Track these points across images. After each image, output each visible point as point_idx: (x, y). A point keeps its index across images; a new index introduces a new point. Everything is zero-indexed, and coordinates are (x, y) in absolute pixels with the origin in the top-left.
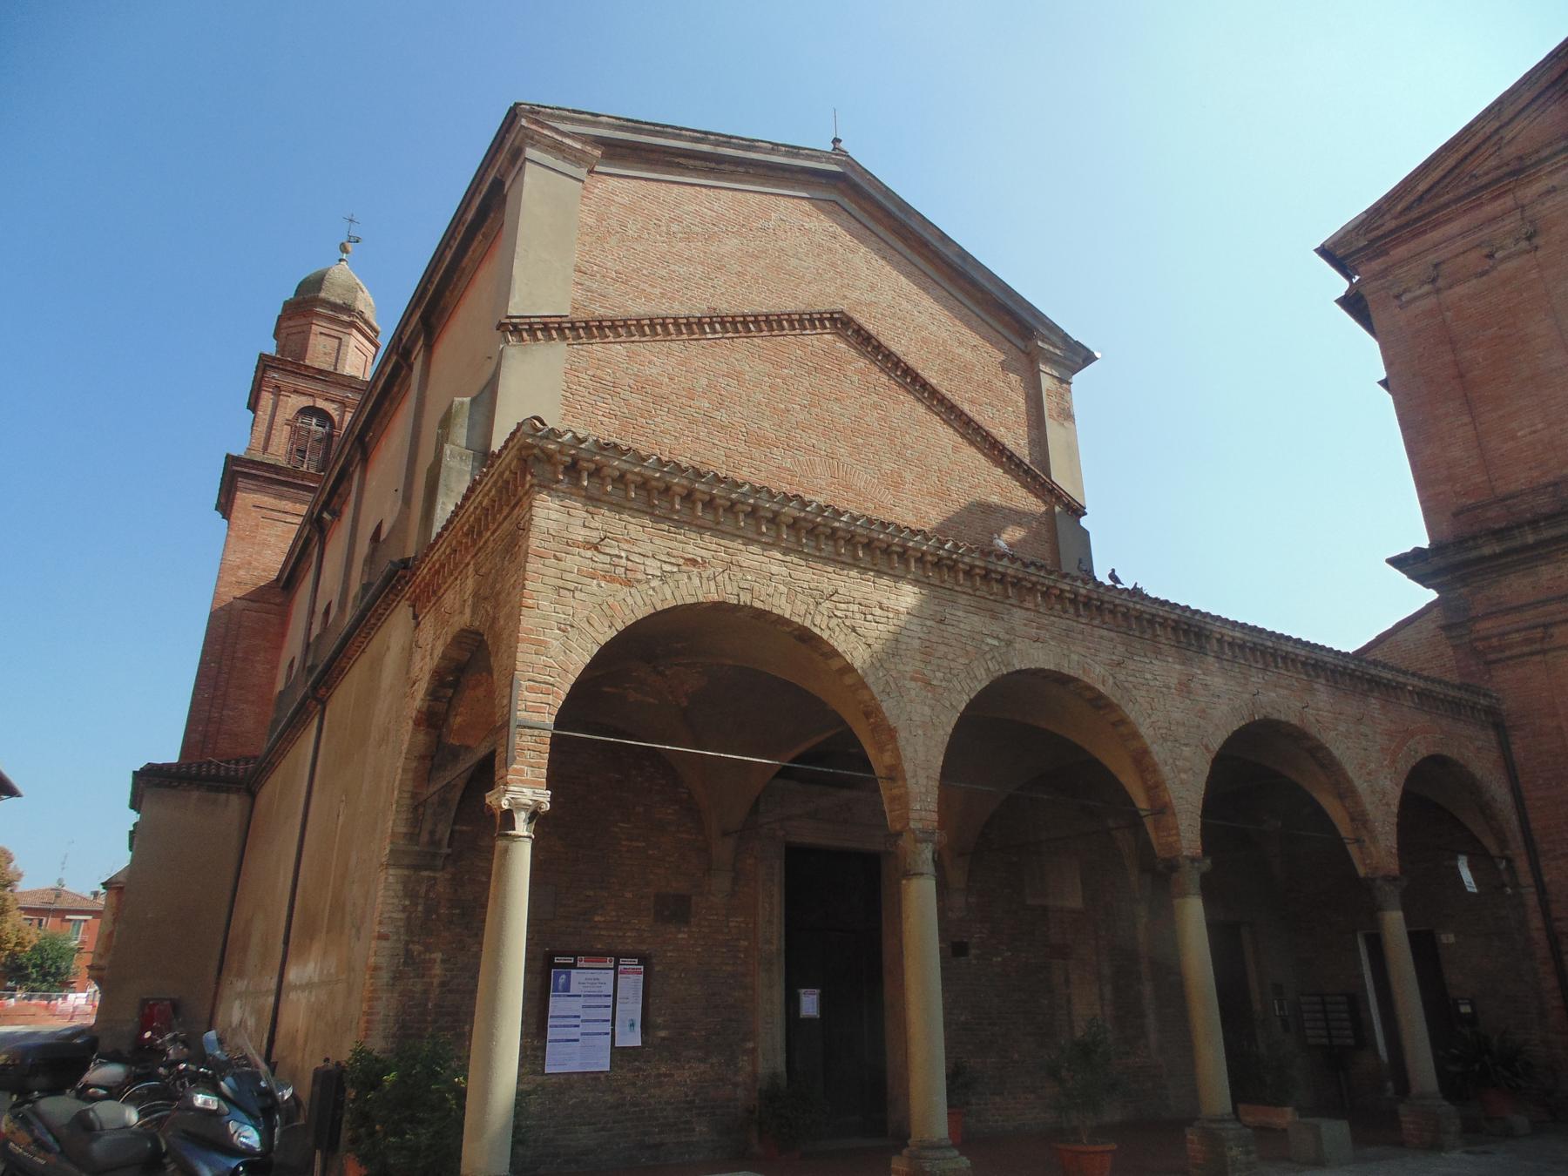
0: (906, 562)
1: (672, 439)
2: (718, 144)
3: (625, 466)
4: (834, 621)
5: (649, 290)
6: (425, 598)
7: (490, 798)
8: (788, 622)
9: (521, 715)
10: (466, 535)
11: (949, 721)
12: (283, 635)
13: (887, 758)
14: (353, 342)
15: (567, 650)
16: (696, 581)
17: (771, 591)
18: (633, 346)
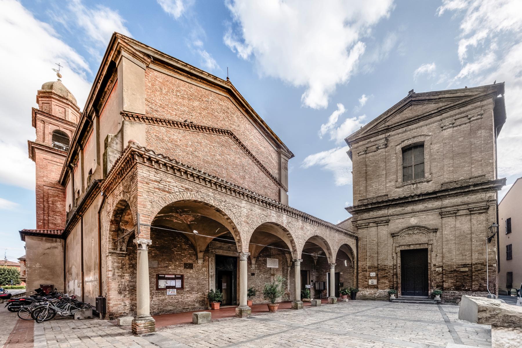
0: (244, 196)
1: (182, 156)
2: (191, 69)
4: (225, 208)
6: (108, 190)
7: (134, 241)
8: (214, 207)
9: (141, 222)
10: (118, 174)
11: (252, 231)
12: (65, 198)
13: (238, 238)
14: (70, 111)
15: (152, 207)
16: (189, 194)
18: (168, 129)
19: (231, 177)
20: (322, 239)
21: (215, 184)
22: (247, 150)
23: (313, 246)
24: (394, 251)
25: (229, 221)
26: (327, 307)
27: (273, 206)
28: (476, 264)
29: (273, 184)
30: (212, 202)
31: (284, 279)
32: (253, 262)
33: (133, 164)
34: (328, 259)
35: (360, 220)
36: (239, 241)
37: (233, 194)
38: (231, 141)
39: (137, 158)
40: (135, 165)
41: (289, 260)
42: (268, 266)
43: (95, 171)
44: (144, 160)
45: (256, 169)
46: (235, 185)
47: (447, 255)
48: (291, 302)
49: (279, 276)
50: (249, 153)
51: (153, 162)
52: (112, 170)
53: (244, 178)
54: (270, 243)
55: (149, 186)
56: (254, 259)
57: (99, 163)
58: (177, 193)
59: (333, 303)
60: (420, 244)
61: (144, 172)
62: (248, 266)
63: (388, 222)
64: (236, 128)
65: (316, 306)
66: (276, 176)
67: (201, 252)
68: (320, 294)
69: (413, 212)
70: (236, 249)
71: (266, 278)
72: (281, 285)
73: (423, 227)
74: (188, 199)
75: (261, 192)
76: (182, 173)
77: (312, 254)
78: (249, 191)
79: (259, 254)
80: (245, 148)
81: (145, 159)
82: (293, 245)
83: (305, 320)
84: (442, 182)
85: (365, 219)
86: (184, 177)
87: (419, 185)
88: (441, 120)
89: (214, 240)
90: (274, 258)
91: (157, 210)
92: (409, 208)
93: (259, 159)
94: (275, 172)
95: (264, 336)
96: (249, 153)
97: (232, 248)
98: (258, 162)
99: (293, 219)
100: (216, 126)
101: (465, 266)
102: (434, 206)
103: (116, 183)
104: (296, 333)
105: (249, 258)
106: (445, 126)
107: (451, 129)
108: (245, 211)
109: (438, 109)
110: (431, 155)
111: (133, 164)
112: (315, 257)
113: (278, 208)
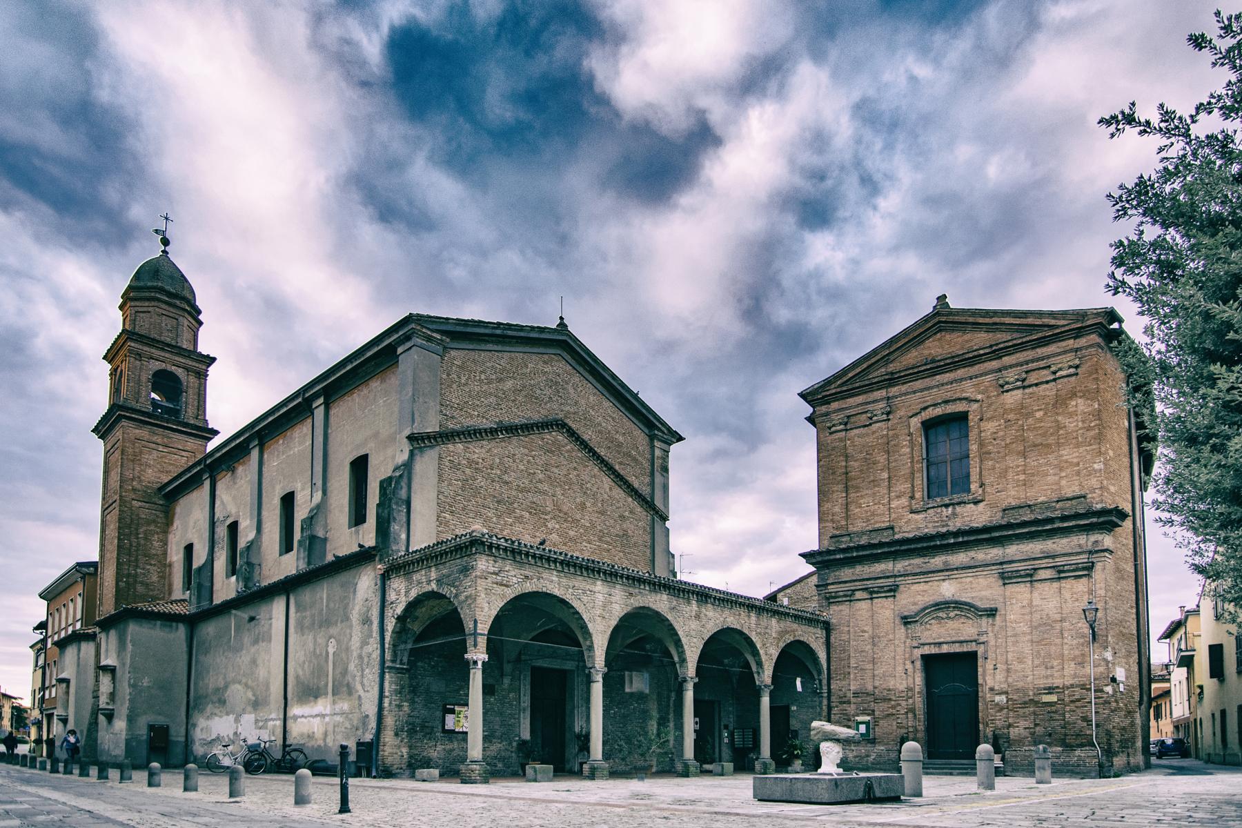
47: (1016, 666)
60: (961, 642)
88: (1000, 370)
107: (1019, 392)
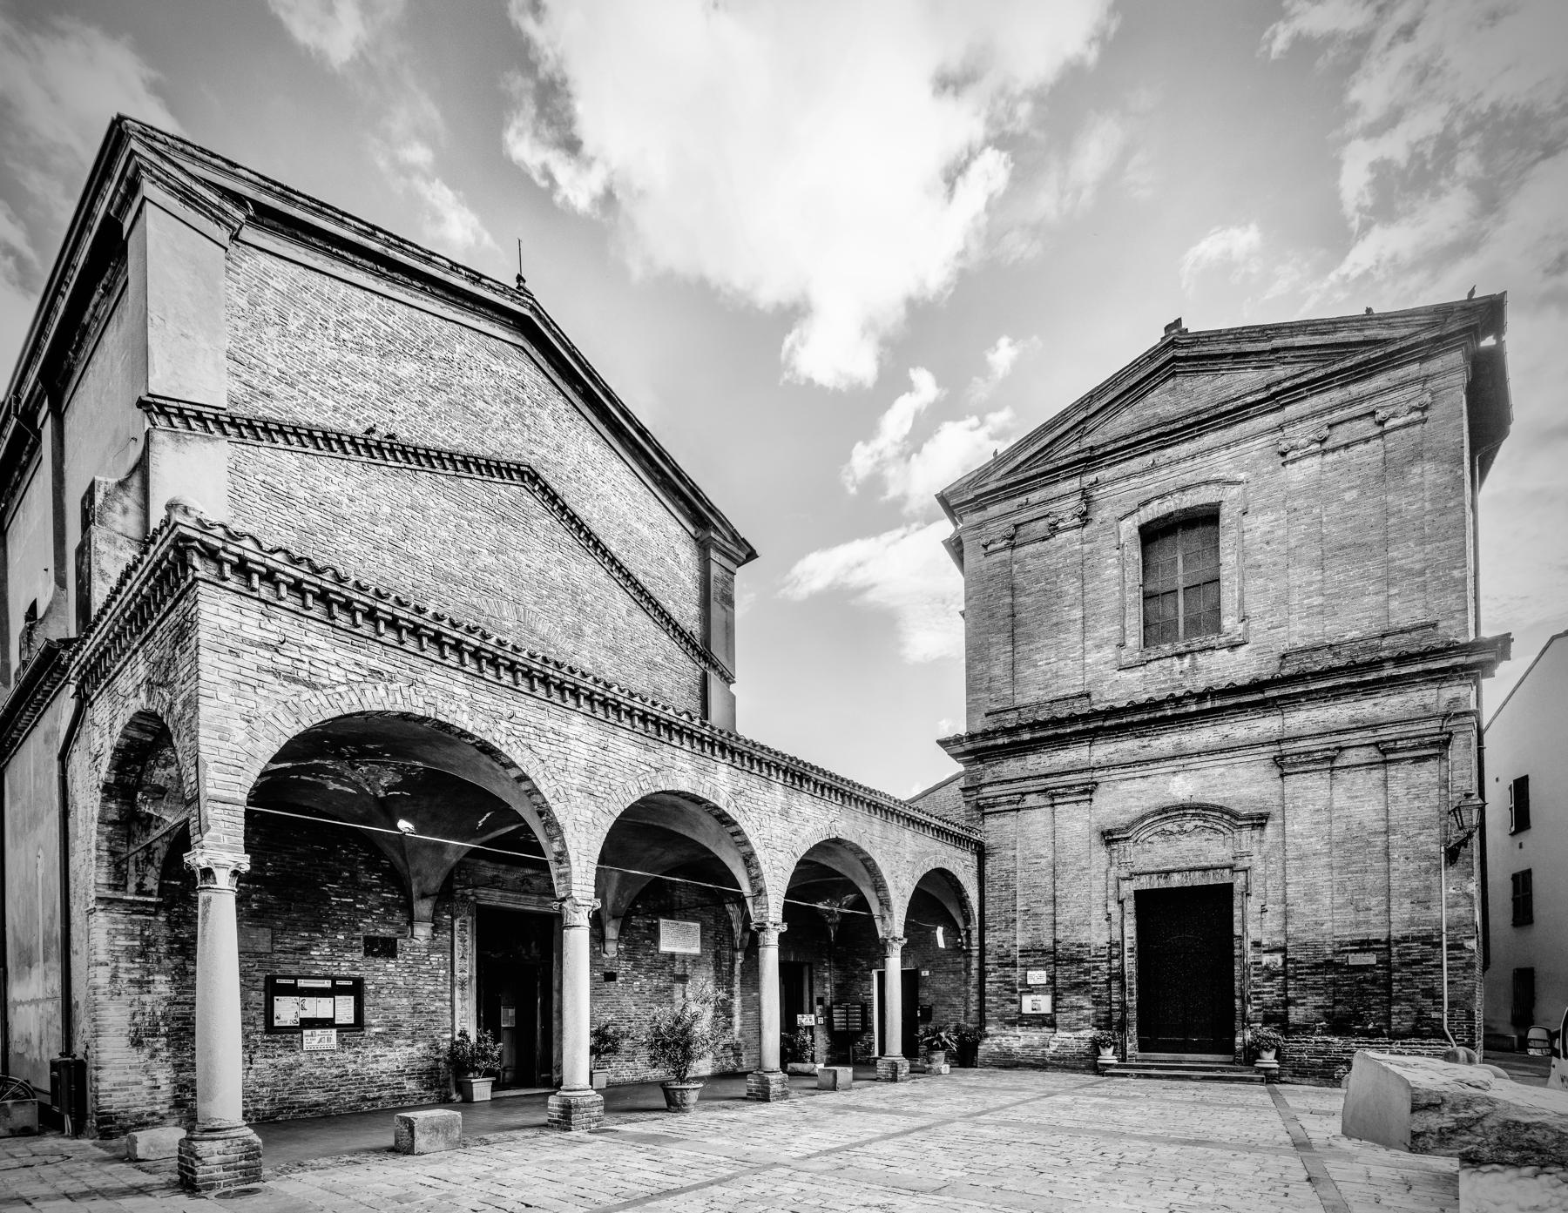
0: (577, 698)
1: (358, 559)
3: (300, 575)
4: (511, 740)
5: (320, 399)
6: (95, 677)
7: (188, 858)
8: (471, 736)
9: (212, 792)
10: (128, 621)
11: (607, 823)
13: (556, 847)
16: (382, 692)
17: (453, 708)
19: (532, 632)
20: (857, 850)
21: (476, 655)
22: (589, 536)
23: (824, 876)
24: (1111, 892)
25: (525, 786)
26: (873, 1094)
27: (680, 733)
28: (1405, 939)
29: (681, 656)
30: (463, 721)
31: (722, 995)
32: (611, 932)
33: (184, 585)
34: (878, 923)
35: (990, 784)
36: (562, 857)
37: (541, 691)
38: (530, 500)
39: (196, 562)
40: (190, 586)
41: (737, 927)
42: (665, 947)
43: (49, 611)
44: (221, 570)
45: (622, 601)
46: (545, 659)
47: (1301, 907)
48: (744, 1075)
49: (703, 983)
50: (597, 544)
51: (255, 577)
52: (107, 605)
53: (579, 635)
54: (668, 862)
55: (239, 661)
56: (612, 923)
57: (61, 582)
58: (339, 689)
59: (894, 1080)
60: (1205, 869)
61: (223, 612)
62: (592, 947)
63: (1089, 790)
64: (551, 457)
65: (834, 1088)
66: (692, 625)
67: (424, 896)
68: (851, 1049)
69: (1180, 755)
70: (551, 886)
71: (658, 990)
72: (709, 1014)
73: (1214, 808)
74: (381, 708)
75: (638, 685)
76: (359, 616)
77: (820, 906)
78: (596, 681)
79: (633, 904)
80: (580, 527)
81: (227, 567)
82: (754, 872)
83: (797, 1141)
84: (1284, 647)
85: (1011, 781)
86: (366, 629)
87: (1201, 659)
88: (1281, 428)
89: (473, 853)
90: (686, 919)
91: (267, 748)
92: (1165, 742)
93: (631, 567)
94: (687, 613)
95: (651, 1197)
96: (594, 544)
97: (535, 882)
98: (628, 576)
99: (754, 779)
100: (478, 450)
101: (1364, 945)
102: (1255, 733)
103: (124, 651)
104: (762, 1187)
105: (597, 921)
106: (1293, 448)
107: (1317, 460)
108: (581, 753)
109: (1268, 387)
110: (1244, 553)
111: (184, 585)
112: (831, 913)
113: (701, 741)
